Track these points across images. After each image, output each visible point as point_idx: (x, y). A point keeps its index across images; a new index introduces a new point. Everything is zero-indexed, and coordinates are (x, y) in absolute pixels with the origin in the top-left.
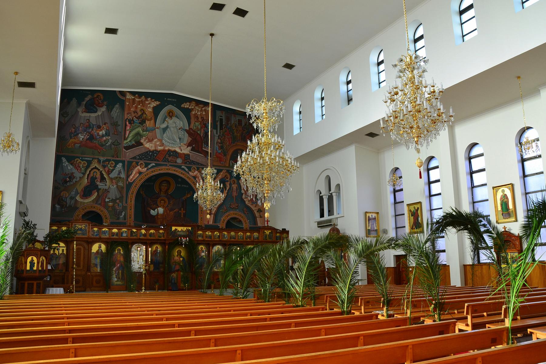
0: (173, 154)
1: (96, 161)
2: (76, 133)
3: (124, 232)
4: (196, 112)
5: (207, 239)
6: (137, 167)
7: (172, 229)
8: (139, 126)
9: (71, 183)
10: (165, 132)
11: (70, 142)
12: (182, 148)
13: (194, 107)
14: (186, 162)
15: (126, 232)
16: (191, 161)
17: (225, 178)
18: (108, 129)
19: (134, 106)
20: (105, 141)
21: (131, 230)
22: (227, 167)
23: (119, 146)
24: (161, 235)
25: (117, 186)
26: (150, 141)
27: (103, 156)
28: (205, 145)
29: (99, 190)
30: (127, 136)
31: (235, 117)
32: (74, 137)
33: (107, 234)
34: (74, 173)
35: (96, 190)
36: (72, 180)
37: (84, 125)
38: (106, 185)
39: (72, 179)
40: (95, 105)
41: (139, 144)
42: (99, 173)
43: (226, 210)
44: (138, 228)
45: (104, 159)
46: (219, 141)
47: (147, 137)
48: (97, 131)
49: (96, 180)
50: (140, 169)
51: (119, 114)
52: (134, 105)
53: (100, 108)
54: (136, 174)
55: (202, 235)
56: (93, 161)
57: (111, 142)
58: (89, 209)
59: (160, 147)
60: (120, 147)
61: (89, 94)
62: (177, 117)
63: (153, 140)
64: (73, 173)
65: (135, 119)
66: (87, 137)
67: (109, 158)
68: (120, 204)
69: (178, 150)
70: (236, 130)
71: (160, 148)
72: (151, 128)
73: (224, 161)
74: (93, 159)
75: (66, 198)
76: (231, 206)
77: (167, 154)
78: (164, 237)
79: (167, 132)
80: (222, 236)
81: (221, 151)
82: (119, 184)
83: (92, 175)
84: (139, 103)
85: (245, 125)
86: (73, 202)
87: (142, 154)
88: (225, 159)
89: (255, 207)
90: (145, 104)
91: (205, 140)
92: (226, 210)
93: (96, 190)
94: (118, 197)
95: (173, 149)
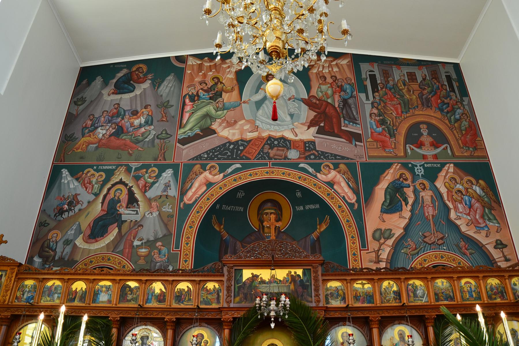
0: (279, 143)
1: (123, 169)
2: (93, 127)
3: (104, 289)
4: (321, 69)
5: (358, 305)
6: (202, 173)
7: (241, 276)
8: (208, 104)
9: (71, 214)
10: (261, 108)
11: (79, 143)
12: (296, 130)
13: (316, 63)
14: (309, 156)
15: (108, 288)
16: (320, 152)
17: (401, 179)
18: (150, 114)
19: (201, 74)
20: (143, 134)
21: (122, 284)
23: (168, 139)
24: (210, 297)
25: (159, 214)
26: (230, 124)
27: (137, 160)
28: (346, 122)
29: (122, 224)
30: (184, 121)
31: (399, 69)
32: (88, 133)
33: (56, 295)
34: (79, 194)
35: (116, 224)
36: (72, 208)
37: (110, 113)
38: (137, 213)
39: (73, 206)
40: (132, 82)
41: (208, 132)
42: (125, 191)
43: (416, 249)
44: (143, 275)
46: (375, 111)
48: (131, 119)
49: (119, 205)
50: (210, 177)
51: (172, 89)
52: (201, 72)
53: (139, 84)
54: (200, 186)
55: (340, 292)
56: (116, 171)
57: (155, 134)
58: (98, 262)
59: (251, 134)
60: (170, 141)
61: (125, 68)
63: (236, 122)
64: (76, 195)
65: (201, 93)
66: (112, 132)
67: (147, 162)
68: (164, 250)
69: (289, 135)
71: (250, 136)
72: (232, 103)
73: (393, 146)
74: (118, 166)
75: (57, 243)
76: (426, 240)
77: (265, 144)
78: (218, 302)
79: (263, 107)
80: (407, 291)
81: (383, 129)
82: (164, 210)
83: (111, 195)
84: (210, 68)
85: (424, 79)
86: (68, 249)
88: (393, 144)
89: (487, 236)
90: (221, 69)
91: (344, 112)
92: (416, 249)
93: (116, 224)
94: (161, 236)
95: (278, 135)
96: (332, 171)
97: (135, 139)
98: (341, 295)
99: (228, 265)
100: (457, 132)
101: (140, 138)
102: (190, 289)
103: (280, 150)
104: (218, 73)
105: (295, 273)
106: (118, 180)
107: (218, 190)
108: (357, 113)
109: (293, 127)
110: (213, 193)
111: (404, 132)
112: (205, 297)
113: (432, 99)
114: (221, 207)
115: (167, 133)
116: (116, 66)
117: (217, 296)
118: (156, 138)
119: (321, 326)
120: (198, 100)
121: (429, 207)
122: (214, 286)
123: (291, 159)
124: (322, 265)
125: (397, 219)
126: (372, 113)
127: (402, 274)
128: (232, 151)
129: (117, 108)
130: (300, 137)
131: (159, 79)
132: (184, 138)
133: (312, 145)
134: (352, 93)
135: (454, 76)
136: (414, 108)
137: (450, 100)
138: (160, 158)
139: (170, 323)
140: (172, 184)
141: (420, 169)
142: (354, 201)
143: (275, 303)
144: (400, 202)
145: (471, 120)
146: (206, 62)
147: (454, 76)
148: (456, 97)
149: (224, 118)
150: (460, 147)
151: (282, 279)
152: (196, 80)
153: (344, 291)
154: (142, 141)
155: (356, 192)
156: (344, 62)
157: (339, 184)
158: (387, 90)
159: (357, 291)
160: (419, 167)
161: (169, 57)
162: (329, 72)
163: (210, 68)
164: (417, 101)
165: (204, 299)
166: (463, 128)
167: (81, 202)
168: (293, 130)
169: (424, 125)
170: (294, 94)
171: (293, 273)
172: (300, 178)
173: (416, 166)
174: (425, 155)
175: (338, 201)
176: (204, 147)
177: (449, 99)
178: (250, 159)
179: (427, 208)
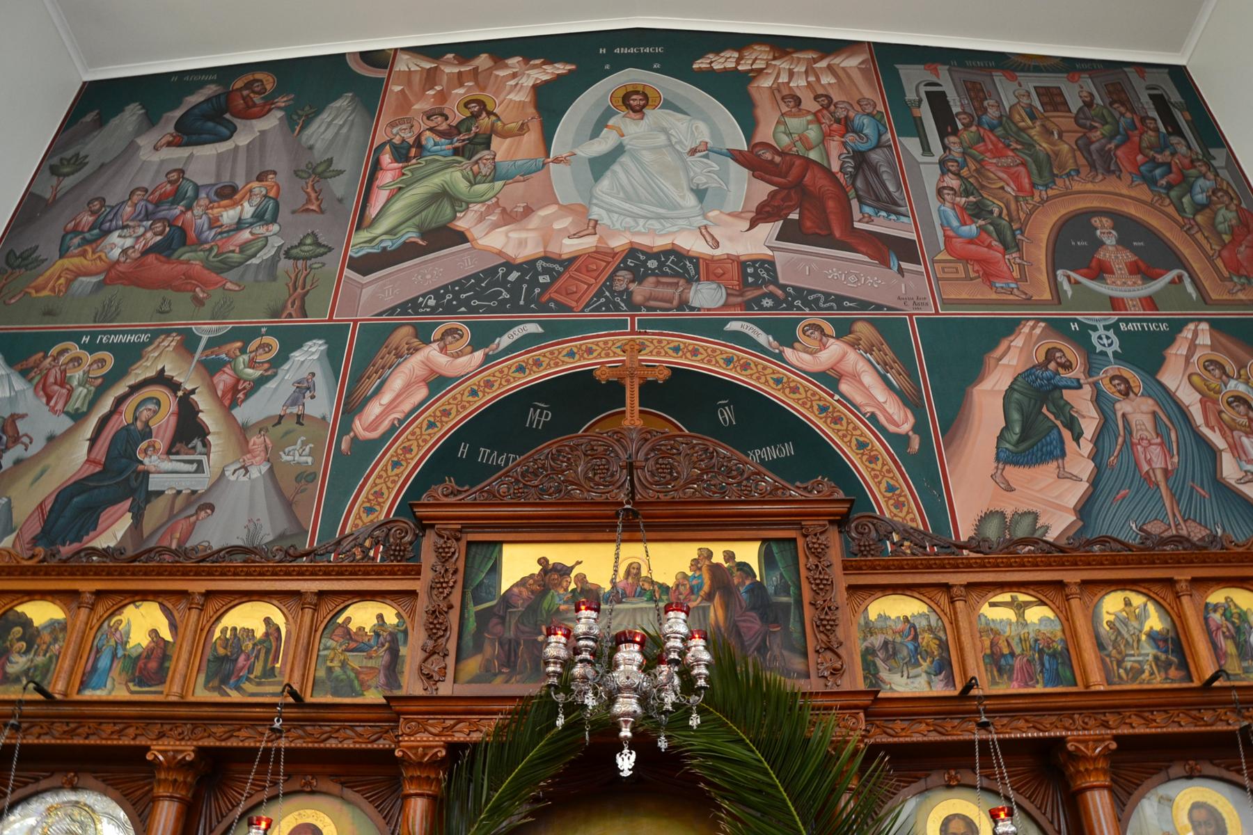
0: (661, 265)
1: (171, 342)
4: (784, 78)
6: (417, 350)
7: (496, 569)
8: (448, 165)
10: (608, 173)
11: (48, 273)
12: (715, 231)
13: (768, 65)
16: (790, 290)
17: (1052, 366)
19: (431, 92)
20: (243, 247)
22: (1042, 304)
24: (356, 661)
25: (271, 470)
26: (510, 217)
28: (867, 209)
29: (148, 501)
30: (373, 211)
31: (1014, 79)
32: (79, 246)
34: (23, 416)
35: (127, 503)
38: (200, 469)
42: (169, 404)
45: (217, 330)
46: (953, 182)
47: (497, 202)
48: (212, 208)
49: (144, 445)
51: (344, 130)
52: (432, 88)
53: (248, 122)
54: (407, 387)
55: (926, 639)
56: (150, 348)
57: (280, 248)
60: (324, 265)
61: (212, 82)
62: (669, 105)
63: (528, 211)
67: (247, 322)
69: (694, 245)
70: (1038, 128)
71: (570, 247)
72: (520, 163)
73: (1016, 274)
74: (155, 334)
77: (618, 269)
79: (614, 172)
80: (1210, 634)
81: (981, 228)
82: (285, 458)
85: (1089, 104)
87: (454, 284)
88: (1016, 268)
90: (493, 78)
91: (859, 184)
94: (270, 538)
95: (660, 243)
96: (831, 340)
97: (220, 261)
98: (929, 653)
99: (439, 525)
100: (1206, 238)
101: (236, 257)
102: (278, 630)
103: (664, 284)
104: (483, 89)
105: (729, 556)
106: (151, 373)
107: (465, 398)
108: (899, 187)
109: (705, 222)
110: (447, 407)
111: (1044, 237)
112: (336, 664)
113: (1119, 153)
114: (473, 453)
115: (317, 243)
116: (187, 78)
117: (387, 658)
118: (282, 256)
119: (854, 784)
120: (419, 156)
121: (1151, 444)
122: (380, 617)
123: (699, 309)
124: (841, 522)
125: (1050, 481)
126: (944, 188)
127: (1178, 561)
128: (515, 289)
129: (178, 180)
130: (728, 248)
131: (307, 108)
132: (369, 254)
133: (767, 270)
134: (880, 135)
135: (1174, 96)
136: (1068, 175)
137: (1173, 154)
138: (290, 310)
139: (169, 769)
140: (320, 381)
141: (1108, 338)
142: (906, 428)
143: (639, 658)
144: (1055, 431)
145: (1243, 205)
146: (448, 63)
147: (1174, 96)
148: (1189, 147)
149: (494, 200)
150: (1223, 279)
151: (671, 582)
152: (416, 107)
153: (942, 634)
154: (240, 264)
155: (911, 401)
156: (851, 62)
157: (856, 377)
158: (982, 131)
159: (997, 633)
160: (1101, 332)
161: (344, 55)
162: (807, 87)
163: (460, 79)
164: (1075, 157)
165: (330, 670)
166: (1221, 227)
167: (25, 440)
168: (704, 231)
169: (1104, 220)
170: (707, 140)
171: (718, 558)
172: (729, 361)
173: (1095, 329)
174: (1117, 299)
175: (856, 428)
176: (428, 277)
177: (1167, 153)
178: (571, 309)
179: (1145, 448)
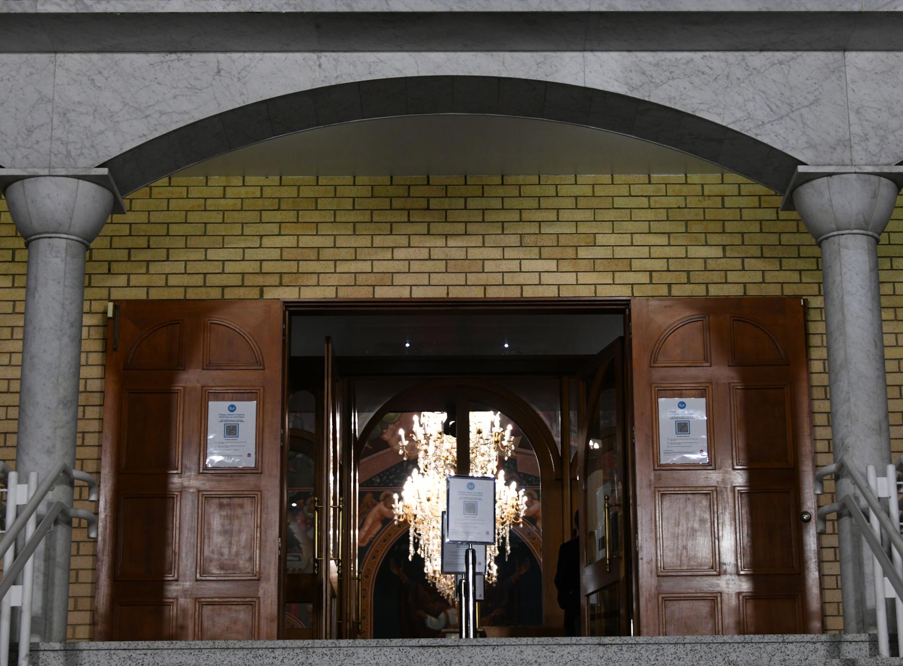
38: (300, 560)
54: (374, 522)
87: (387, 470)
96: (536, 501)
